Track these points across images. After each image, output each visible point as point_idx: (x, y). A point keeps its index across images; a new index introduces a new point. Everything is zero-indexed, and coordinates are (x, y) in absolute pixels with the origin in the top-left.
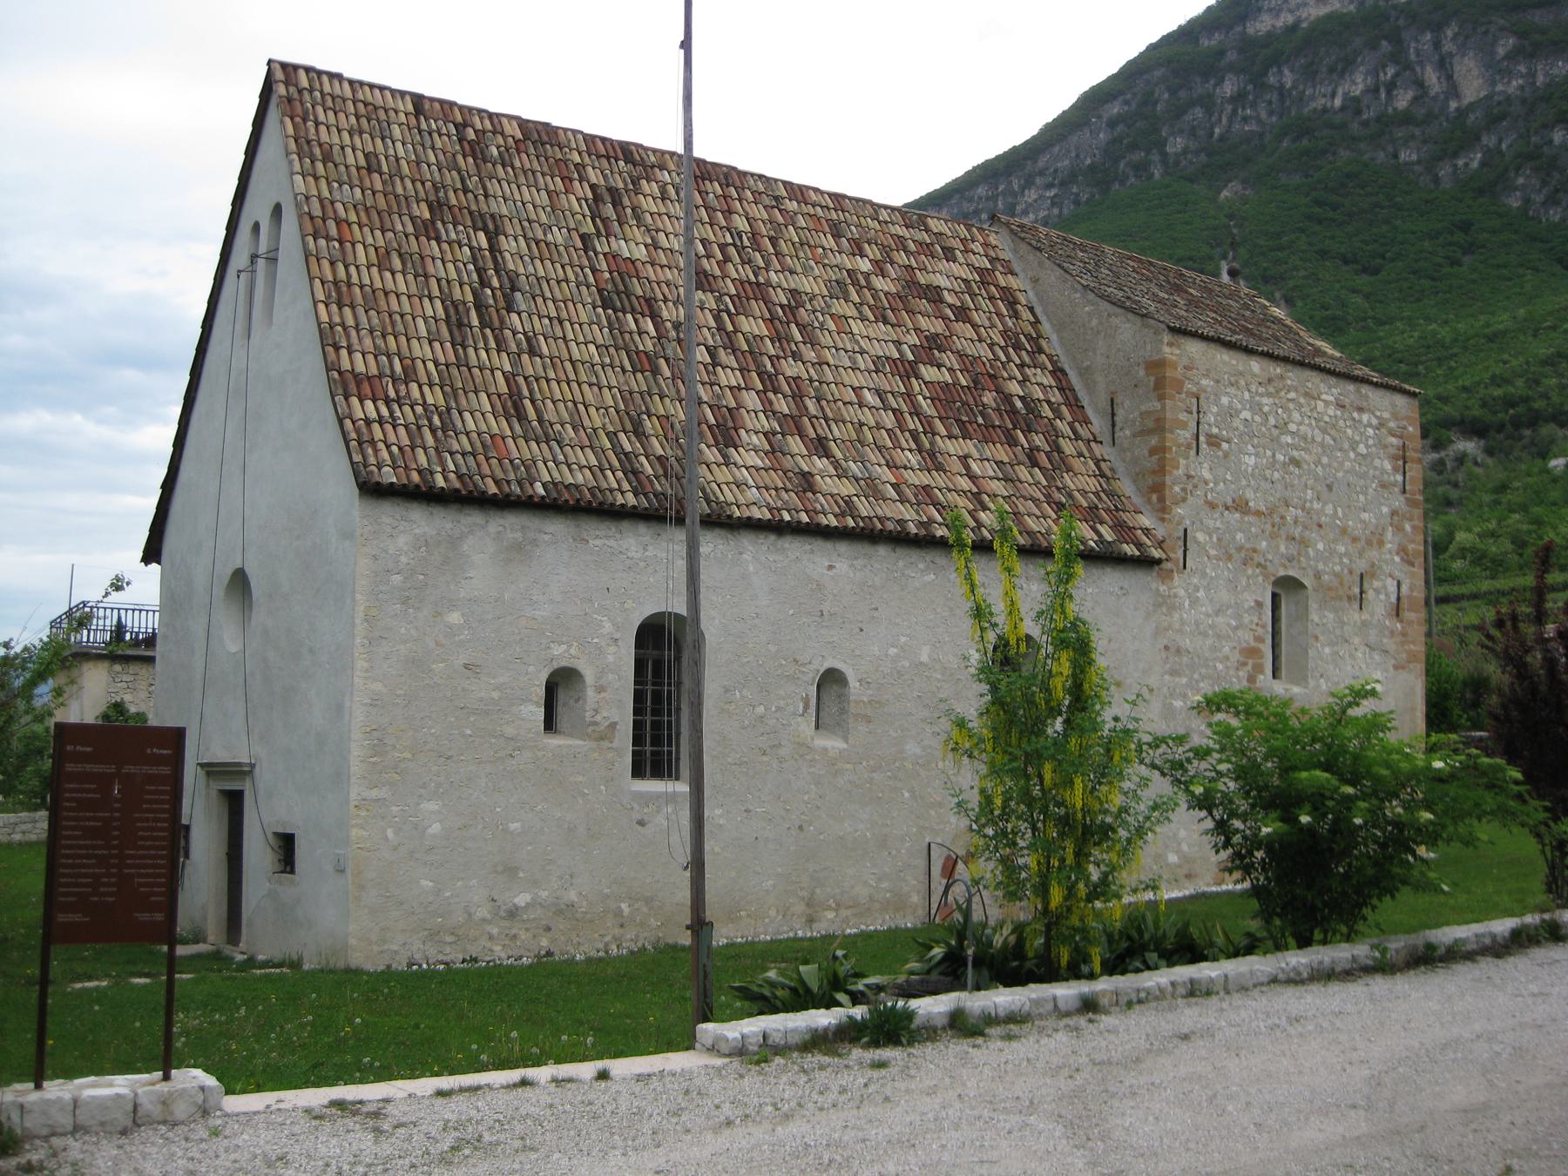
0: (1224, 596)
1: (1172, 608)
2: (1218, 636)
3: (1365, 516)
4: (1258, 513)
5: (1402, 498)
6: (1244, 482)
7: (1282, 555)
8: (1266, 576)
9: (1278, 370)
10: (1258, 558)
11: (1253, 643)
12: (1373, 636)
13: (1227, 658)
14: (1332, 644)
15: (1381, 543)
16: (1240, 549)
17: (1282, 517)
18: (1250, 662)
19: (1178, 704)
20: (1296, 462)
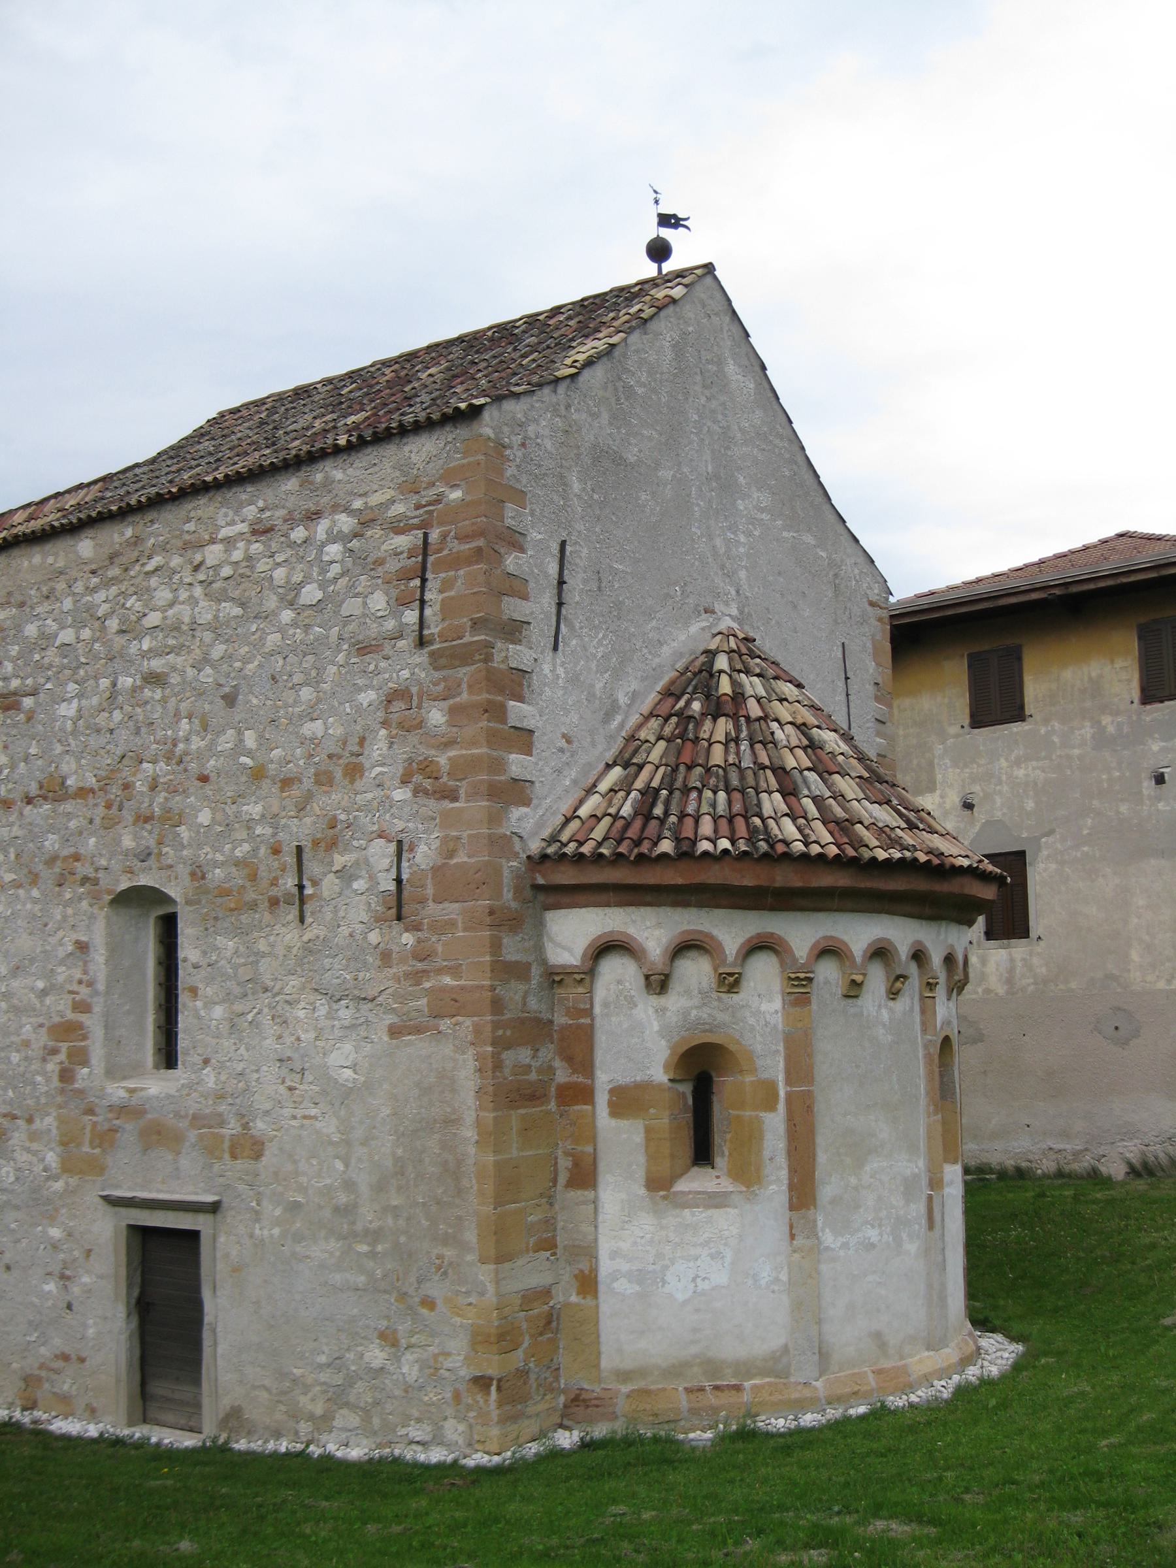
4: (83, 792)
5: (421, 658)
6: (59, 749)
7: (126, 853)
8: (95, 897)
9: (129, 532)
10: (82, 869)
11: (70, 1015)
12: (336, 972)
13: (27, 1044)
14: (228, 998)
15: (354, 771)
16: (52, 860)
17: (127, 786)
18: (64, 1046)
20: (155, 679)
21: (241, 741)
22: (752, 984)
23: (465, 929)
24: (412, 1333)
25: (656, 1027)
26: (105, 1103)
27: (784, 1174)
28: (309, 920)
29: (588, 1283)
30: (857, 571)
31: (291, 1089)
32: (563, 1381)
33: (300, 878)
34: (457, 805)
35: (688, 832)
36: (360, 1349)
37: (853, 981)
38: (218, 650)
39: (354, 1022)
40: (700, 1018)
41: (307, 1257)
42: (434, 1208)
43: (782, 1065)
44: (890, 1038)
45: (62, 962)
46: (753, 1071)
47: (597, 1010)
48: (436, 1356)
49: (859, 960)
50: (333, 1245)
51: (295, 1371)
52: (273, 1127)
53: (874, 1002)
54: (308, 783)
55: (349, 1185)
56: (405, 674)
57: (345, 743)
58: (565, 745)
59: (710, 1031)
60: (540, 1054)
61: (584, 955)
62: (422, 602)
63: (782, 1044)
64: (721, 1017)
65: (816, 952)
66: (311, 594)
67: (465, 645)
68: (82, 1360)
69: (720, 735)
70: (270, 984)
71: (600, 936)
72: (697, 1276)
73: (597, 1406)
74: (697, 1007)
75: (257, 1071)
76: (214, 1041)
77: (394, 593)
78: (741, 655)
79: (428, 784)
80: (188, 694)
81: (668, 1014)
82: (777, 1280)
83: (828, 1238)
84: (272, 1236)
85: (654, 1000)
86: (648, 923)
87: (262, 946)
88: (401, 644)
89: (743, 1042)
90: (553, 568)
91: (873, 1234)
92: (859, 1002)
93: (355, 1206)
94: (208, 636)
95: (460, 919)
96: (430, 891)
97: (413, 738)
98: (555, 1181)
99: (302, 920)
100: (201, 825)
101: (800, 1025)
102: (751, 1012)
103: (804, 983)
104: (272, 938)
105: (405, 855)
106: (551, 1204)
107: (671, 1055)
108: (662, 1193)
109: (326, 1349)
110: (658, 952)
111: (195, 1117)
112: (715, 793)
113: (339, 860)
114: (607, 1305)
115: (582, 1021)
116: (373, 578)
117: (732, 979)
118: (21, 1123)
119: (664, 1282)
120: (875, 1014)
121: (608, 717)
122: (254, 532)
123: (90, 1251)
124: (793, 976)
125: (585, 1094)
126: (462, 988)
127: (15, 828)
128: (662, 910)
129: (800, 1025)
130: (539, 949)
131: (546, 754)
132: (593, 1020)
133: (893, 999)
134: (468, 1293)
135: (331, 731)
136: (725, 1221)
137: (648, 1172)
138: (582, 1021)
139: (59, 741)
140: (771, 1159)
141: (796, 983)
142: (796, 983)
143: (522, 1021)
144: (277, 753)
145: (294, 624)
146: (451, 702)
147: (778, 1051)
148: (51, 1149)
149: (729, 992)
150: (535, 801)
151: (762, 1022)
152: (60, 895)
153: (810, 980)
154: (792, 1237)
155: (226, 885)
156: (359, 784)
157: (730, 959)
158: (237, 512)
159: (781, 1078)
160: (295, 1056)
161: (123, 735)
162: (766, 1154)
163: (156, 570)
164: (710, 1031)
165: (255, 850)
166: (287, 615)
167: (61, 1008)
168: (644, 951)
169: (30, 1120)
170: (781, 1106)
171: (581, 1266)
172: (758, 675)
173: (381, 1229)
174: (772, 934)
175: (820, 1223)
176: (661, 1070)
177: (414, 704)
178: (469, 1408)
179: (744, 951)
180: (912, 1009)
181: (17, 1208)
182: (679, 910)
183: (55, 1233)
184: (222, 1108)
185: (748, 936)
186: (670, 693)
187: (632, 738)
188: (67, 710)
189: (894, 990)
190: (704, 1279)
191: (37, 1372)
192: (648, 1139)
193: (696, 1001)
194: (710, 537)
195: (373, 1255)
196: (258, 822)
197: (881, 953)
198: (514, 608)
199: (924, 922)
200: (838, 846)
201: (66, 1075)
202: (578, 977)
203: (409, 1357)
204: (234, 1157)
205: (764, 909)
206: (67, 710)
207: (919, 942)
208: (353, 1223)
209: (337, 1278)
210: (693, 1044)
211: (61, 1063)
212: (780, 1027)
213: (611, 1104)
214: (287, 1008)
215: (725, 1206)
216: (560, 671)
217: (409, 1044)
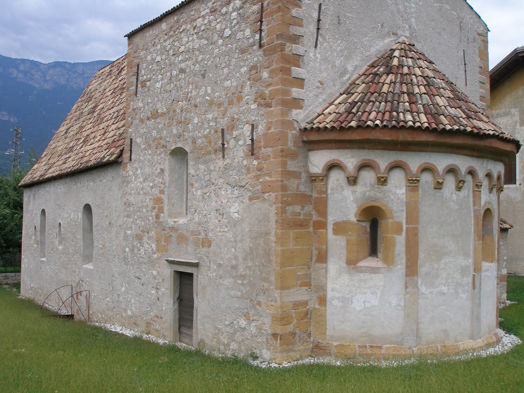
0: (147, 170)
1: (128, 182)
2: (145, 194)
3: (228, 83)
4: (163, 114)
5: (260, 52)
6: (156, 99)
9: (176, 18)
10: (163, 142)
11: (159, 195)
12: (234, 176)
14: (202, 188)
15: (240, 99)
16: (155, 139)
19: (129, 232)
20: (182, 71)
21: (207, 91)
22: (393, 182)
23: (273, 158)
24: (254, 315)
25: (352, 199)
26: (168, 226)
27: (404, 261)
28: (226, 157)
29: (323, 301)
30: (471, 21)
31: (219, 221)
32: (312, 339)
33: (223, 141)
34: (272, 109)
35: (364, 118)
36: (238, 320)
37: (438, 182)
38: (200, 57)
39: (239, 195)
40: (370, 195)
41: (223, 284)
42: (261, 267)
43: (405, 216)
44: (456, 207)
45: (157, 176)
46: (392, 218)
47: (329, 191)
48: (261, 324)
49: (441, 173)
50: (231, 280)
51: (219, 326)
52: (214, 235)
53: (449, 191)
54: (226, 105)
55: (236, 258)
56: (256, 59)
57: (237, 89)
58: (320, 85)
59: (374, 201)
60: (305, 208)
61: (323, 169)
62: (261, 30)
63: (405, 207)
64: (379, 195)
65: (421, 169)
66: (227, 32)
67: (274, 45)
68: (162, 318)
69: (388, 81)
70: (214, 181)
71: (329, 161)
72: (366, 301)
73: (323, 349)
74: (369, 191)
75: (210, 214)
76: (198, 203)
77: (253, 28)
78: (405, 50)
79: (262, 102)
80: (191, 75)
81: (357, 193)
82: (399, 305)
83: (423, 289)
84: (213, 276)
85: (351, 188)
86: (348, 156)
87: (212, 168)
88: (255, 48)
89: (388, 206)
90: (315, 15)
91: (445, 289)
92: (442, 191)
93: (238, 265)
94: (197, 53)
95: (271, 154)
96: (262, 144)
97: (258, 84)
98: (311, 260)
99: (224, 157)
100: (195, 124)
101: (413, 199)
102: (392, 194)
103: (415, 182)
104: (215, 164)
105: (255, 130)
106: (309, 268)
107: (358, 210)
108: (352, 266)
109: (228, 319)
110: (352, 168)
111: (192, 232)
112: (380, 103)
113: (235, 133)
114: (329, 310)
115: (323, 196)
116: (247, 23)
117: (383, 179)
118: (146, 233)
119: (352, 302)
120: (449, 196)
121: (342, 75)
122: (211, 12)
123: (164, 279)
124: (410, 179)
125: (321, 225)
126: (272, 181)
127: (145, 129)
128: (354, 150)
129: (413, 199)
130: (306, 166)
131: (311, 89)
132: (327, 195)
133: (459, 191)
134: (271, 301)
135: (233, 84)
136: (378, 279)
137: (347, 257)
138: (323, 196)
139: (156, 96)
140: (399, 255)
141: (412, 182)
142: (412, 182)
143: (297, 195)
144: (217, 94)
145: (222, 45)
146: (270, 68)
147: (403, 210)
148: (154, 243)
149: (382, 185)
150: (304, 107)
151: (397, 198)
152: (156, 152)
153: (418, 181)
154: (406, 287)
155: (202, 145)
156: (241, 104)
157: (382, 171)
158: (206, 5)
159: (404, 221)
160: (221, 208)
161: (174, 92)
162: (397, 252)
163: (183, 30)
164: (374, 201)
165: (210, 131)
166: (220, 42)
167: (156, 192)
168: (346, 167)
169: (148, 233)
170: (404, 233)
171: (320, 294)
172: (411, 58)
173: (245, 274)
174: (401, 161)
175: (420, 283)
176: (354, 216)
177: (258, 70)
178: (271, 345)
179: (388, 168)
180: (468, 196)
181: (145, 263)
182: (361, 150)
183: (155, 273)
184: (200, 228)
185: (390, 161)
186: (372, 66)
187: (353, 83)
188: (158, 85)
189: (459, 187)
190: (368, 302)
191: (150, 321)
192: (348, 244)
193: (369, 188)
194: (397, 5)
195: (243, 284)
196: (211, 121)
197: (452, 170)
198: (295, 30)
199: (474, 158)
200: (429, 124)
201: (158, 217)
202: (321, 178)
203: (253, 324)
204: (203, 247)
205: (397, 150)
206: (158, 85)
207: (472, 167)
208: (237, 272)
209: (232, 293)
210: (367, 206)
211: (156, 212)
212: (405, 200)
213: (334, 230)
214: (219, 190)
215: (379, 273)
216: (318, 56)
217: (255, 203)
